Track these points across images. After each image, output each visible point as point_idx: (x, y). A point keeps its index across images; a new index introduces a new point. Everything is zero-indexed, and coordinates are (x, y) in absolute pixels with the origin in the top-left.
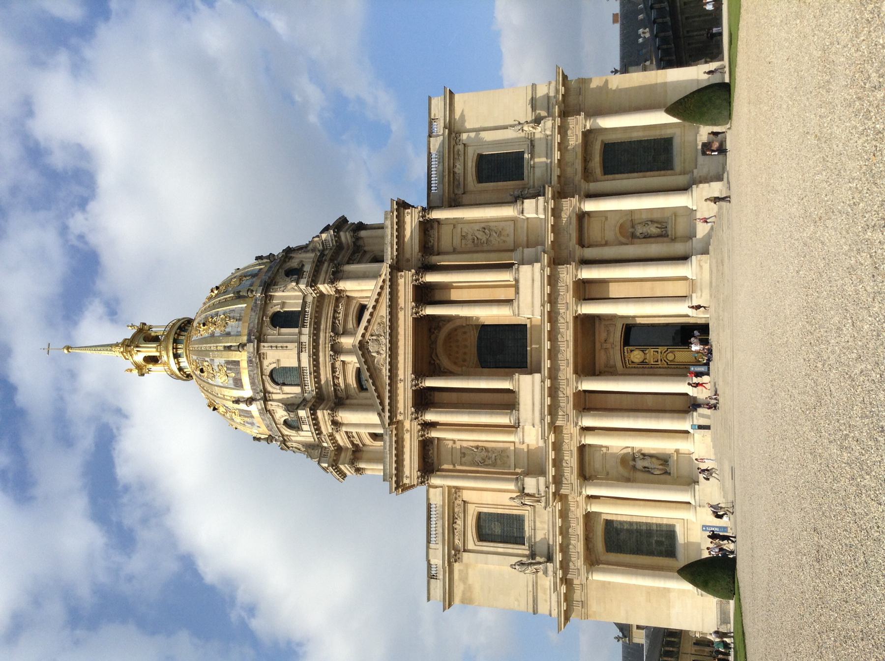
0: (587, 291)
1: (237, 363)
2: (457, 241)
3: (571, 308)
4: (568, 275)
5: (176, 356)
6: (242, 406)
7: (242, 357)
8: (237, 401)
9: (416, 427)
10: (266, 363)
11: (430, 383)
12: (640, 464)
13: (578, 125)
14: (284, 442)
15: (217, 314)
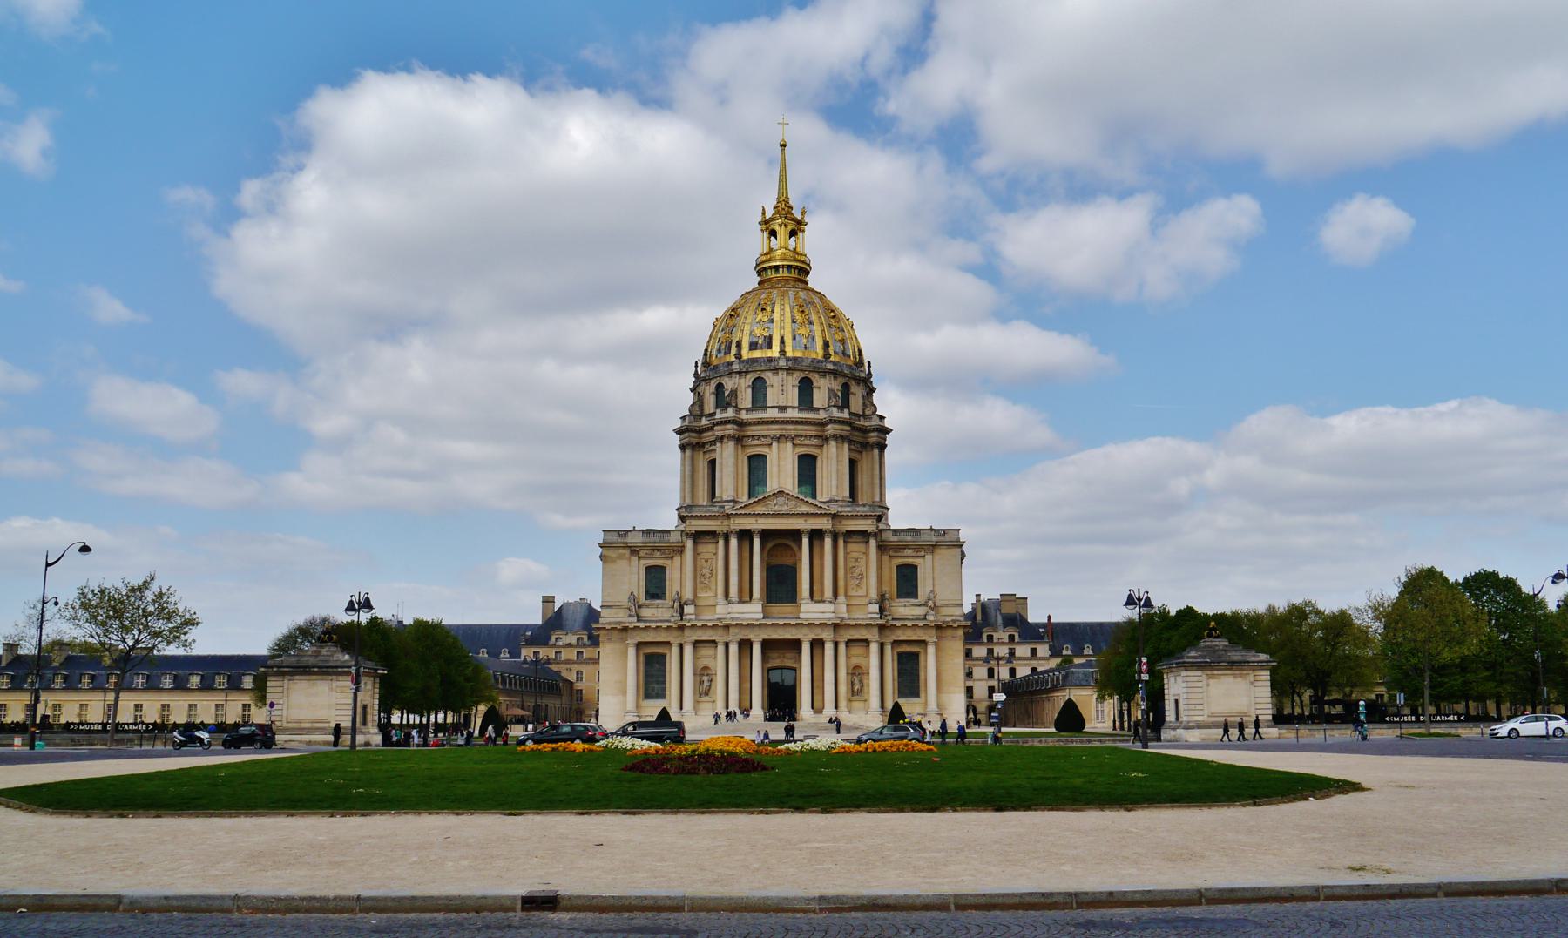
0: (817, 645)
1: (770, 346)
2: (854, 555)
3: (806, 637)
4: (827, 635)
5: (777, 268)
6: (734, 350)
7: (775, 352)
8: (739, 344)
9: (725, 529)
10: (769, 374)
11: (757, 542)
12: (705, 678)
13: (930, 637)
14: (705, 379)
15: (811, 323)
